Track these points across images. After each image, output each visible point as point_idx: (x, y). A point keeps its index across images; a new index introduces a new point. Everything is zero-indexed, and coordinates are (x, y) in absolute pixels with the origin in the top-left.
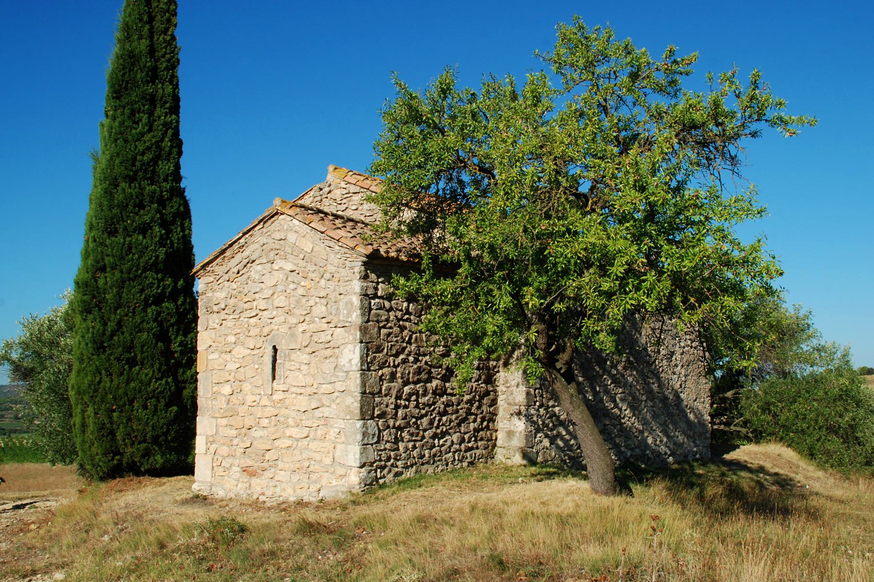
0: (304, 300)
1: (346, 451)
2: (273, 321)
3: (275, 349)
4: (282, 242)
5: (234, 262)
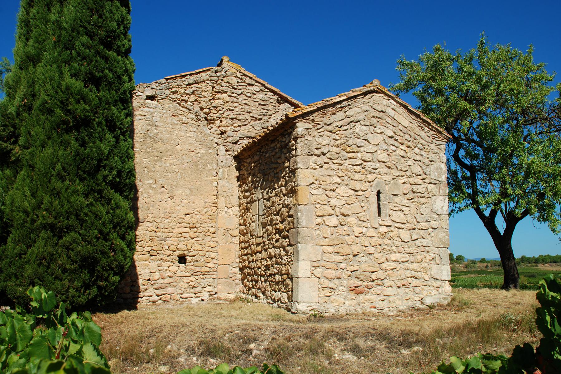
0: (403, 159)
1: (441, 270)
2: (376, 171)
3: (379, 193)
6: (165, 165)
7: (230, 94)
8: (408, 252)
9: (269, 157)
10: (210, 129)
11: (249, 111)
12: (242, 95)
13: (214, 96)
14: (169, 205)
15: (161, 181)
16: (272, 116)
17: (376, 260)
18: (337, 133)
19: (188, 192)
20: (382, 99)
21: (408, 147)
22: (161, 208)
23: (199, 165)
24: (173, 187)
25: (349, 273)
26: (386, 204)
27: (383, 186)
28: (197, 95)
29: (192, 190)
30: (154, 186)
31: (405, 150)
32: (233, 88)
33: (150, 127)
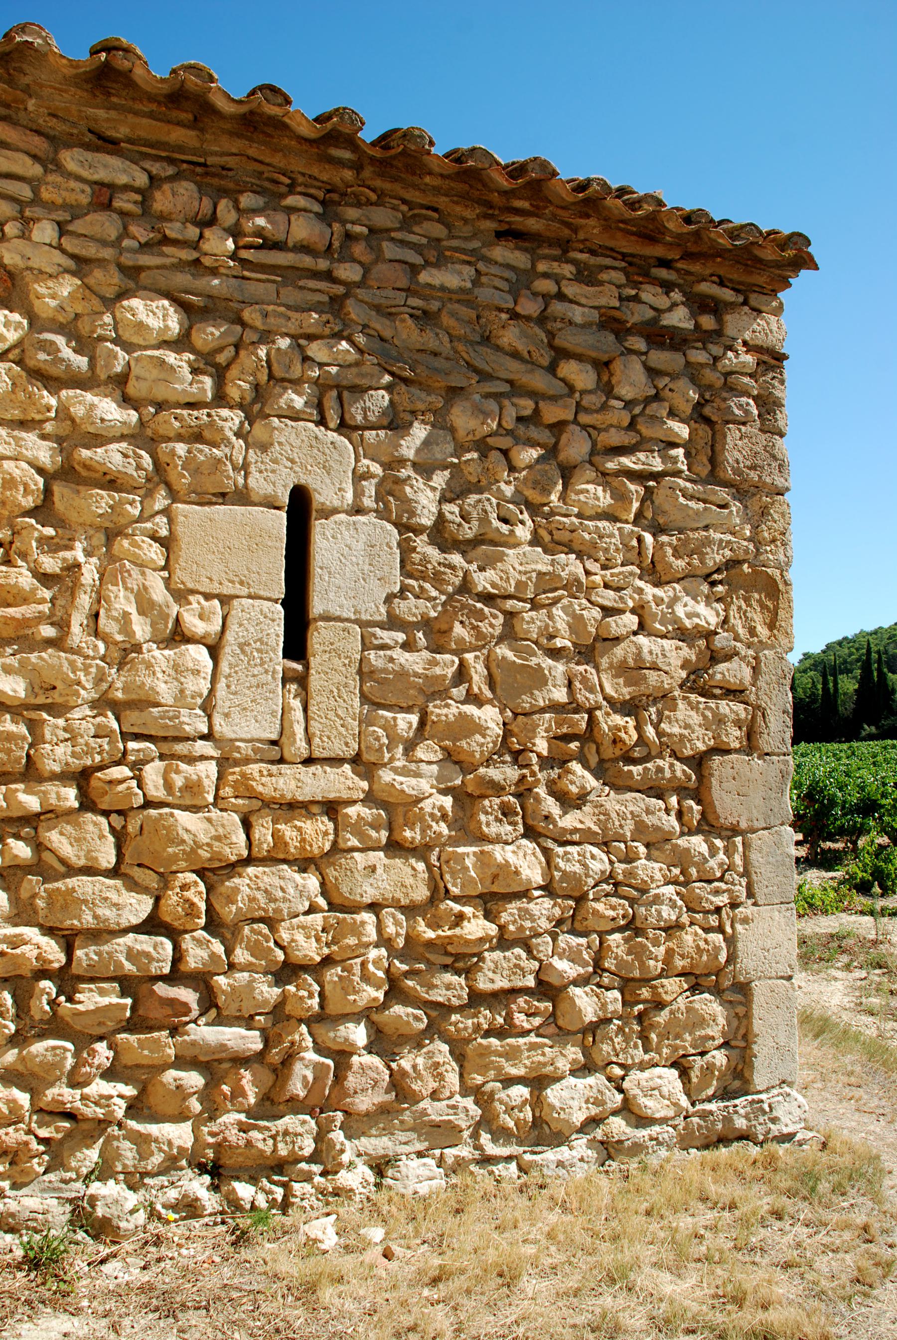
9: (464, 297)
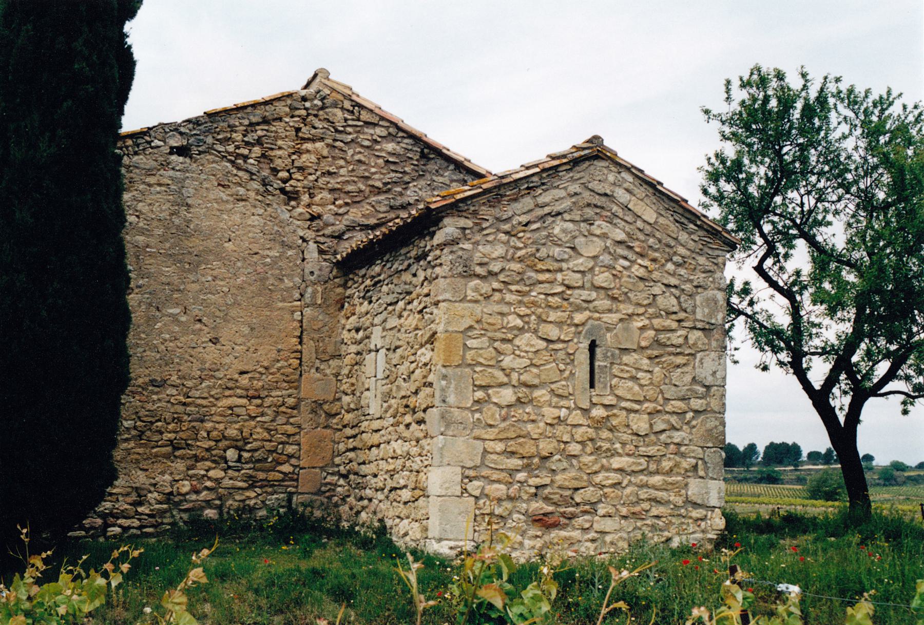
0: (641, 285)
1: (707, 488)
2: (591, 306)
3: (593, 346)
4: (604, 199)
5: (518, 207)
6: (204, 279)
7: (330, 141)
8: (645, 454)
10: (290, 211)
11: (367, 174)
12: (353, 145)
13: (299, 146)
14: (211, 354)
15: (196, 311)
16: (411, 185)
17: (583, 467)
18: (521, 235)
19: (246, 330)
20: (606, 171)
21: (654, 260)
22: (195, 361)
23: (268, 278)
24: (218, 320)
25: (533, 490)
26: (606, 367)
27: (602, 332)
28: (265, 145)
29: (254, 326)
30: (183, 319)
31: (646, 267)
32: (337, 131)
33: (177, 208)
